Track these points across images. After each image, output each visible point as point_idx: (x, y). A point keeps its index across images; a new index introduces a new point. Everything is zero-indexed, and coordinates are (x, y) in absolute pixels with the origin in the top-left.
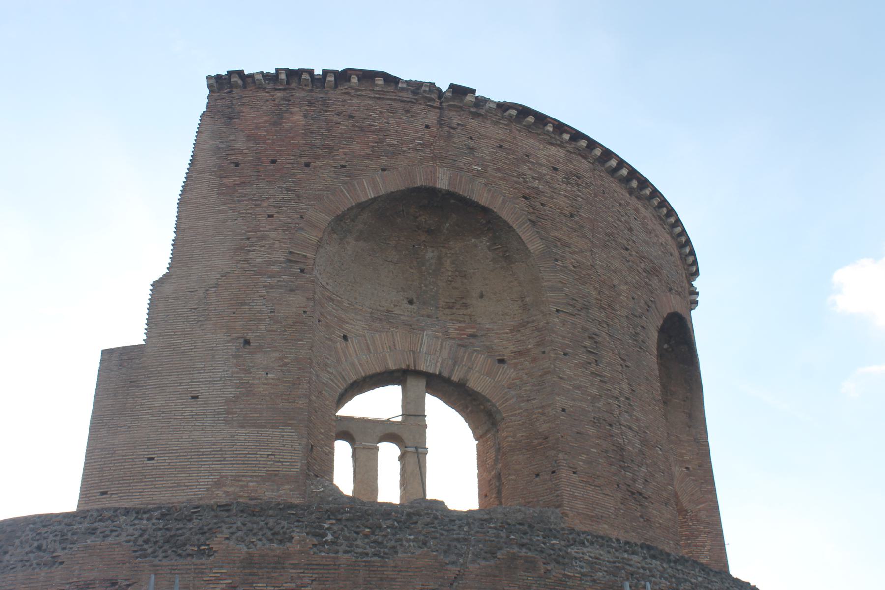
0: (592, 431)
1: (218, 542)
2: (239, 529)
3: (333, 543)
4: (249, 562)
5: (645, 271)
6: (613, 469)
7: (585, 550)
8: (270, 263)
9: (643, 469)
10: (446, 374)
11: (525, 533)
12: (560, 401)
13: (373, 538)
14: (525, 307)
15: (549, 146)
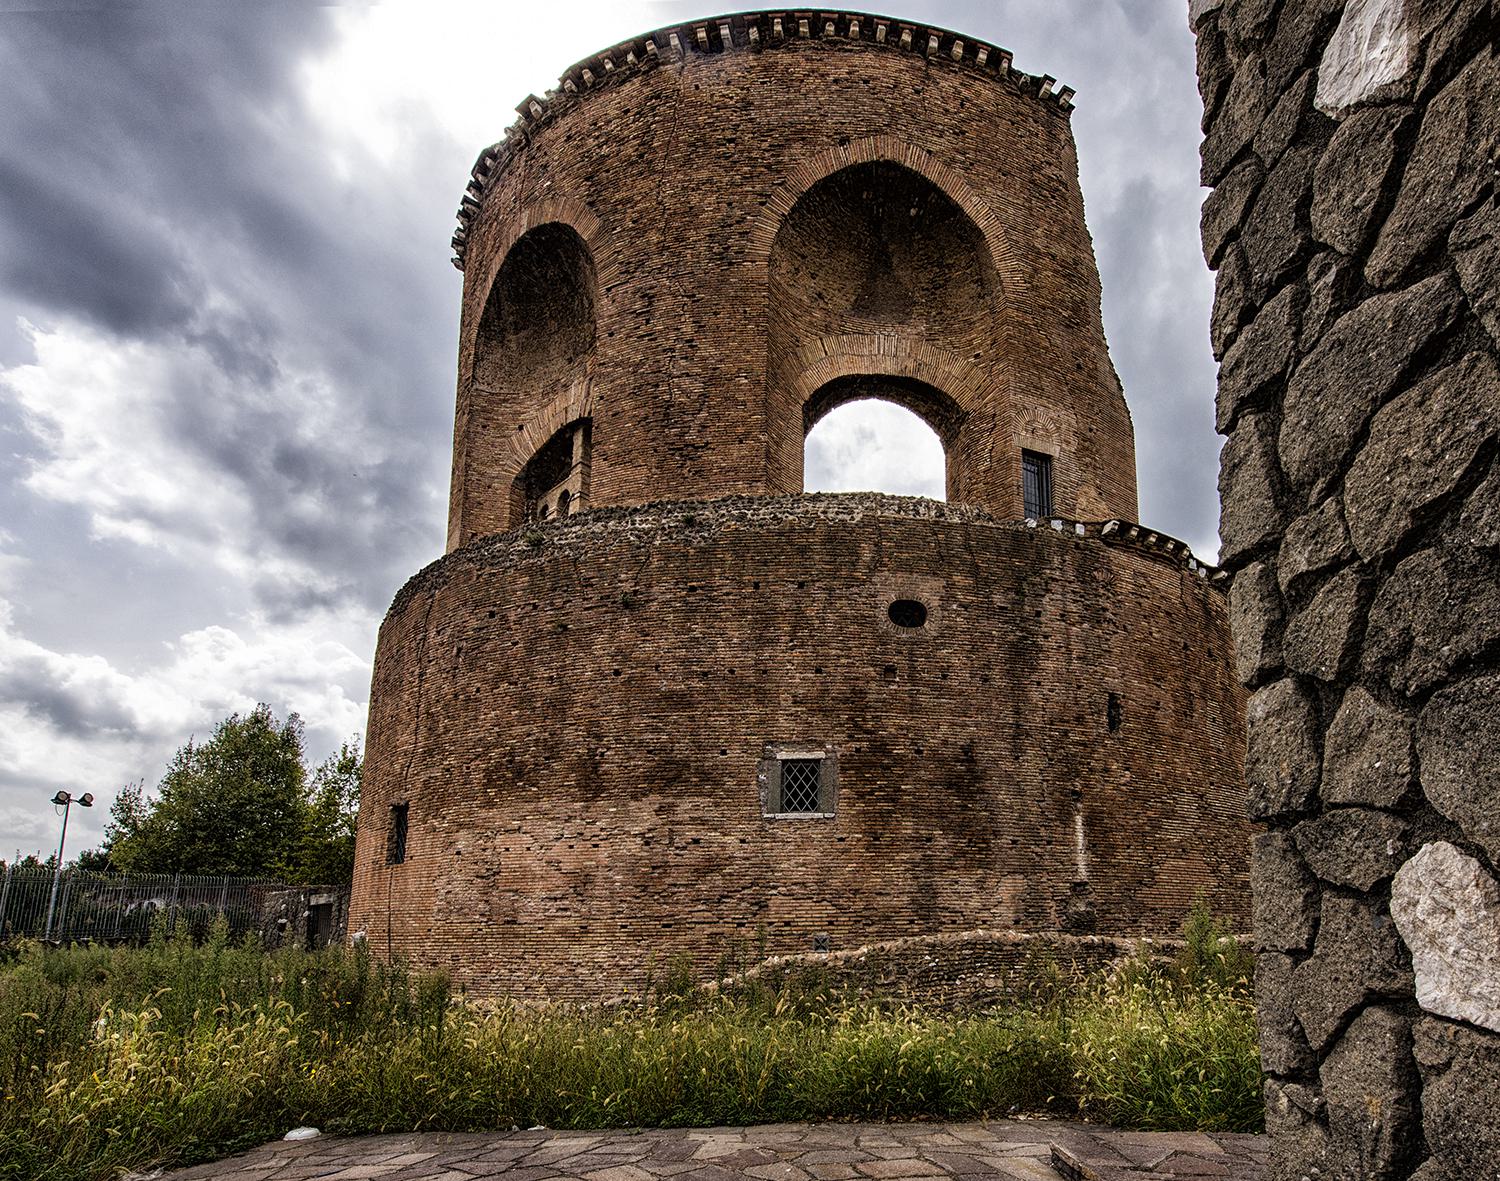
0: (627, 404)
9: (703, 414)
15: (623, 88)
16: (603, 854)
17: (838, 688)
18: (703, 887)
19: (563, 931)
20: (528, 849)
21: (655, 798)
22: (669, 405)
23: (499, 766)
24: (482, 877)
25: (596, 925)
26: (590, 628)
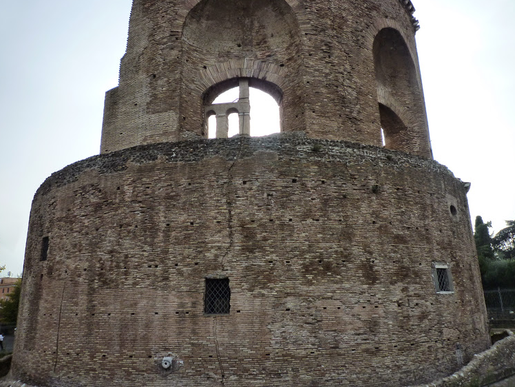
0: (324, 90)
1: (129, 163)
2: (138, 156)
3: (176, 157)
4: (140, 170)
5: (366, 8)
6: (337, 108)
7: (305, 147)
8: (163, 38)
9: (358, 106)
10: (256, 76)
11: (270, 142)
12: (306, 78)
13: (194, 153)
14: (292, 37)
16: (381, 311)
17: (446, 240)
18: (423, 325)
19: (367, 351)
20: (339, 308)
21: (400, 284)
22: (344, 98)
23: (312, 264)
24: (308, 323)
25: (383, 347)
26: (358, 199)
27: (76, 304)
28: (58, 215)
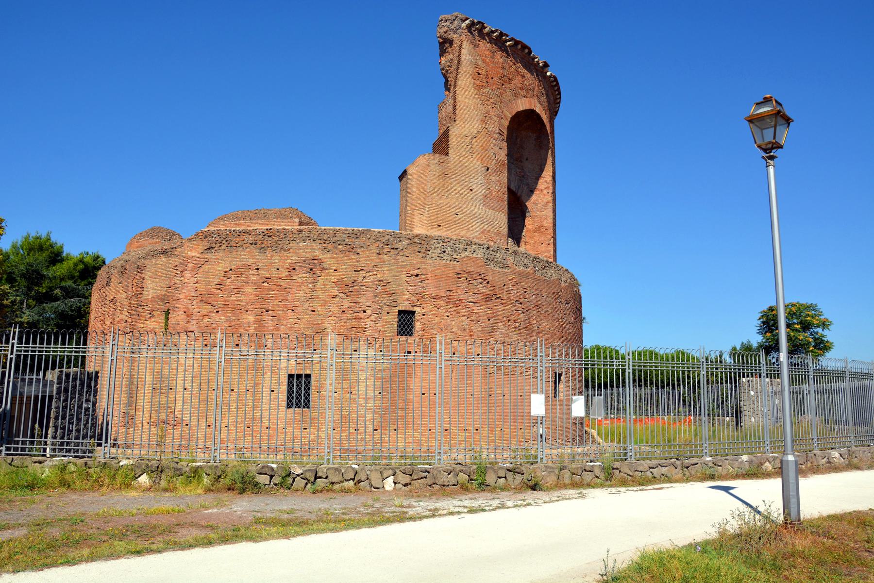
4: (520, 274)
27: (470, 385)
28: (431, 290)
